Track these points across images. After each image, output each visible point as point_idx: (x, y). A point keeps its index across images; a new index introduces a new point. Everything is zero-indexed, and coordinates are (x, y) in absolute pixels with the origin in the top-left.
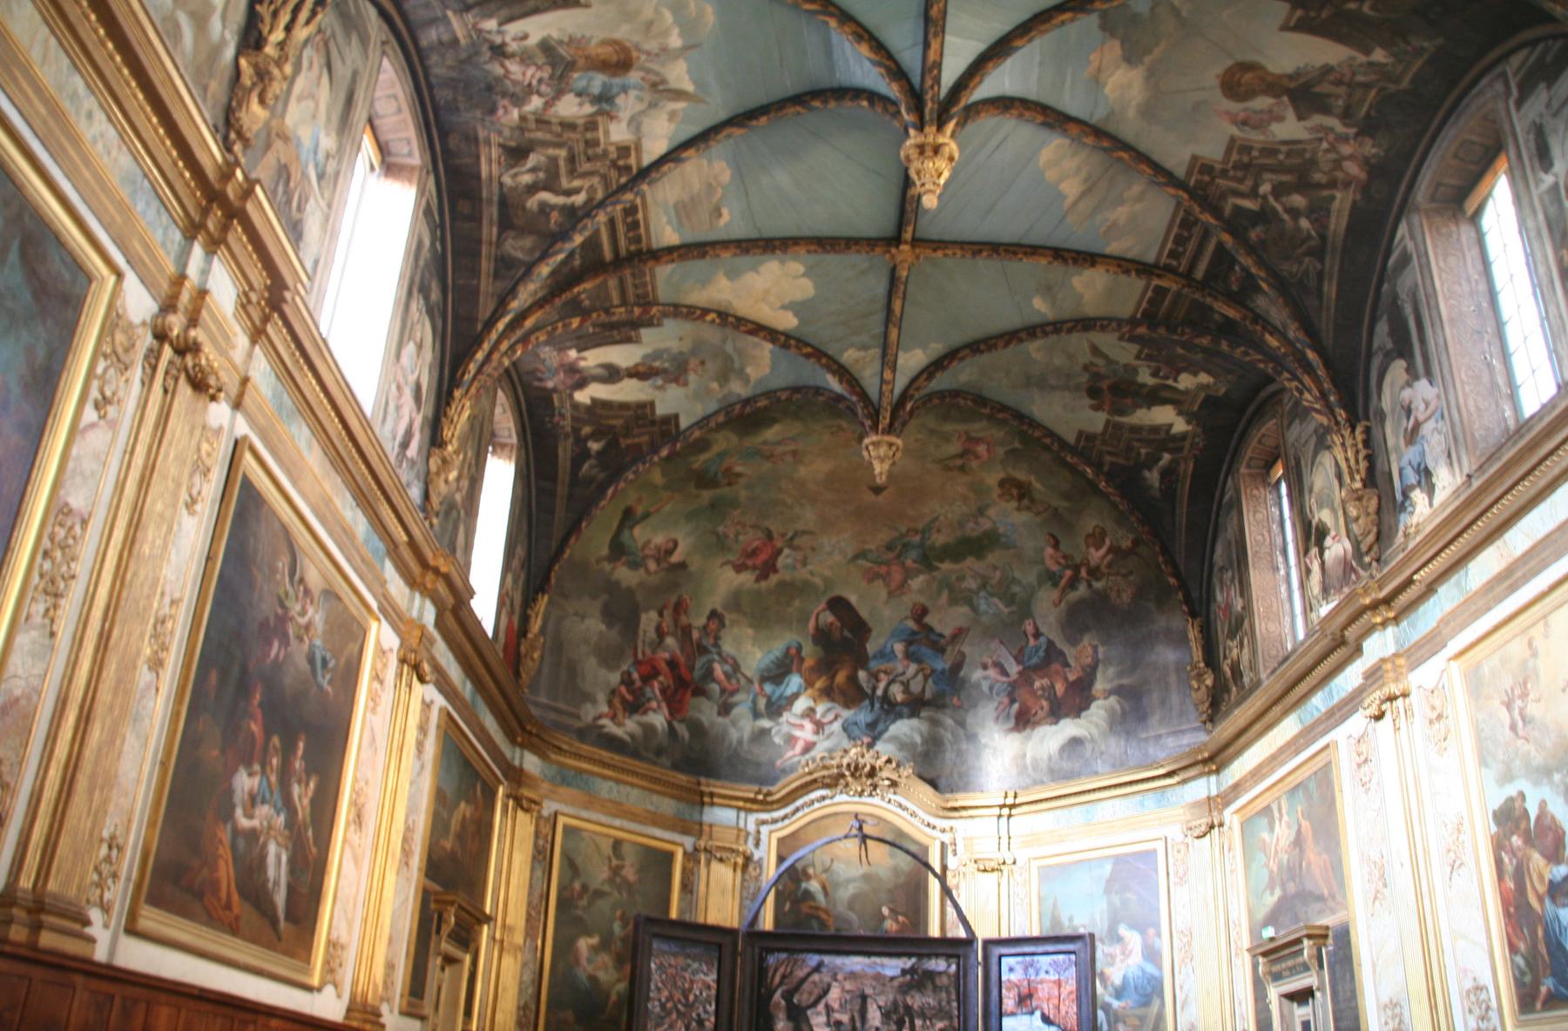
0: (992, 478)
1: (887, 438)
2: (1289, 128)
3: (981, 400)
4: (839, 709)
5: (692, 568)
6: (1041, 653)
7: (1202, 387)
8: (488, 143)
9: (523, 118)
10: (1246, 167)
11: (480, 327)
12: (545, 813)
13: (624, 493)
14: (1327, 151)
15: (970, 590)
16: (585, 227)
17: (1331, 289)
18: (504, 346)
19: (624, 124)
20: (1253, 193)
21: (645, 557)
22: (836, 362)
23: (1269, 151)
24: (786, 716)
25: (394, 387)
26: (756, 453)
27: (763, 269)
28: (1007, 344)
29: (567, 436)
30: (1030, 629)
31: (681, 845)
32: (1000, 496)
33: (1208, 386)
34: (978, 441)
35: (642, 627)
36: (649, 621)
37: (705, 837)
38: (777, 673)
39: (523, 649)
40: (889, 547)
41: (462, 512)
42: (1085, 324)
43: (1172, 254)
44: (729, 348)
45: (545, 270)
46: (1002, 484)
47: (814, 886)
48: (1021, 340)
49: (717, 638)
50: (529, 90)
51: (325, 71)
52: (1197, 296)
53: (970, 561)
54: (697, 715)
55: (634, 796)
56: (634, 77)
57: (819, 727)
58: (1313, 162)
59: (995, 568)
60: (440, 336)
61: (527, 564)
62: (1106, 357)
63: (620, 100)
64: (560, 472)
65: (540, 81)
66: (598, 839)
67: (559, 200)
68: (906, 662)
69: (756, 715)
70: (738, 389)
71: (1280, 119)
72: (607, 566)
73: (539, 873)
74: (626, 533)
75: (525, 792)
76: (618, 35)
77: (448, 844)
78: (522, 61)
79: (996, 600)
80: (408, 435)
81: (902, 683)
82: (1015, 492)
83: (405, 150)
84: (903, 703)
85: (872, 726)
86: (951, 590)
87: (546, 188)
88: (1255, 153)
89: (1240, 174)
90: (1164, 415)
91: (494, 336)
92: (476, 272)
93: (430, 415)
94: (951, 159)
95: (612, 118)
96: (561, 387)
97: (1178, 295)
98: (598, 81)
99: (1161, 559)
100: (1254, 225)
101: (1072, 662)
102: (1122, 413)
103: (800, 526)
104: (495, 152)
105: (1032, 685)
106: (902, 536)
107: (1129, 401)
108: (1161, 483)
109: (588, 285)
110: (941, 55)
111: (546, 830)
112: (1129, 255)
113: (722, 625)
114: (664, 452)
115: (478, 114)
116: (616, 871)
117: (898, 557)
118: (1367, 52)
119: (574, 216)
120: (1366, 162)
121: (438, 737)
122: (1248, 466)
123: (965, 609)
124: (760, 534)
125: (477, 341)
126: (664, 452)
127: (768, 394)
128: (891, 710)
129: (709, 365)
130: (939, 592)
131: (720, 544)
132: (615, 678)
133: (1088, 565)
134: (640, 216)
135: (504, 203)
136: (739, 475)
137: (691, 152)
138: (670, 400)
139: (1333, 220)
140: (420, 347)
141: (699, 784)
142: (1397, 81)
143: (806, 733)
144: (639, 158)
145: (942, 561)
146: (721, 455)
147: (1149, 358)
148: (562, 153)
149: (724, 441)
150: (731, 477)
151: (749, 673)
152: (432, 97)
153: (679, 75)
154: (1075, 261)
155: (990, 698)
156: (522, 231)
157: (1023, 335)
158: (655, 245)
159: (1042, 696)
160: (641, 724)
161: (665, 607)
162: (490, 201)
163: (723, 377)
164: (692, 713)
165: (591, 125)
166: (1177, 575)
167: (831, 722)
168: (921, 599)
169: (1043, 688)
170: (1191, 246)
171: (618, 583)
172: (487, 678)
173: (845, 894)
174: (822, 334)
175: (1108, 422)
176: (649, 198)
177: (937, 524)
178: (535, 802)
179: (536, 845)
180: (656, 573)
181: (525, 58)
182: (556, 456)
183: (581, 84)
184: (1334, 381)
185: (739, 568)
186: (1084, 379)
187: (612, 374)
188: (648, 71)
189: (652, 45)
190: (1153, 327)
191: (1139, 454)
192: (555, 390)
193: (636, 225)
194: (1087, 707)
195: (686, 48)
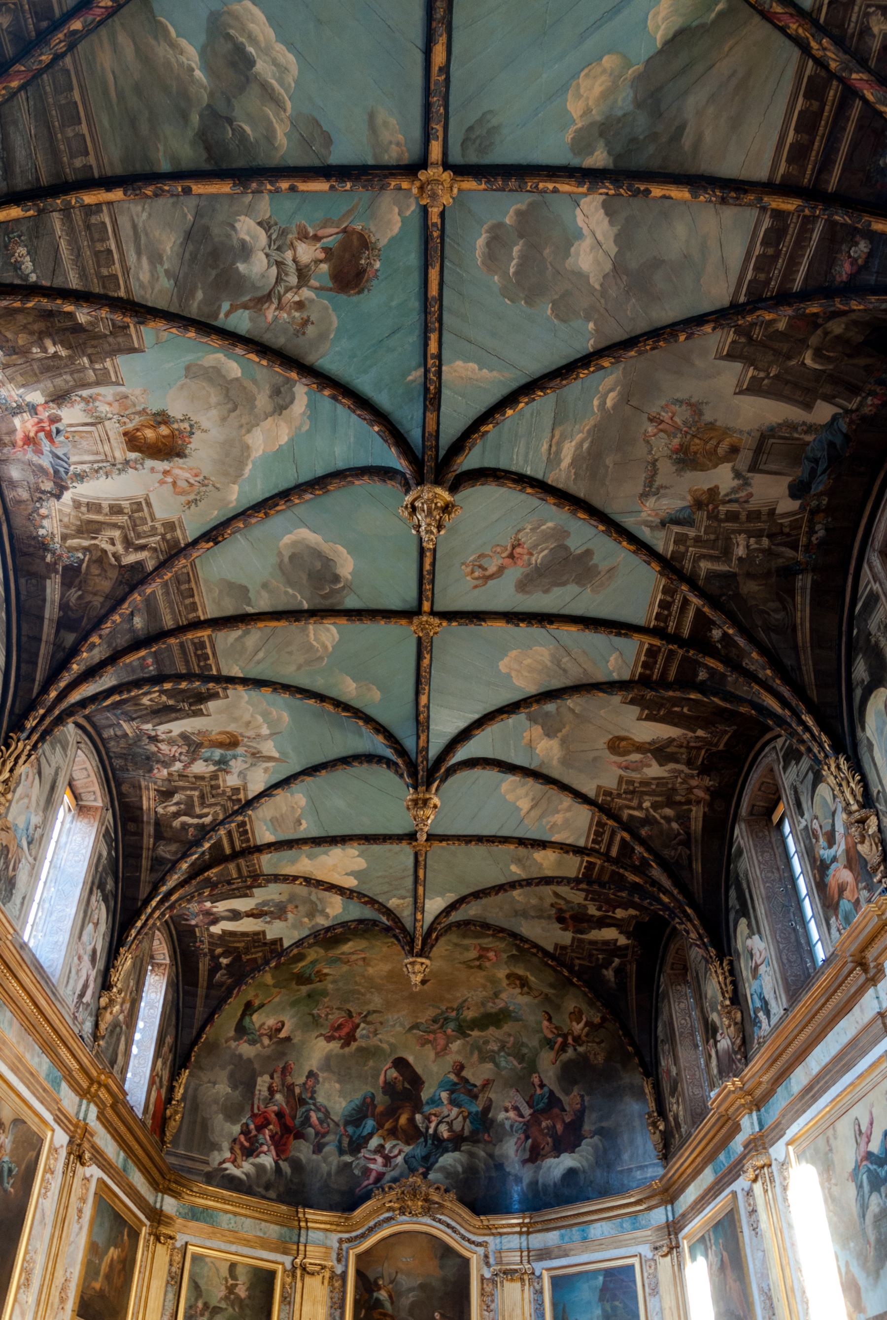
0: (501, 973)
1: (420, 960)
2: (655, 770)
3: (486, 926)
4: (401, 1146)
5: (295, 1041)
6: (546, 1101)
7: (632, 917)
8: (148, 788)
9: (170, 774)
10: (633, 792)
11: (139, 904)
12: (178, 1244)
13: (248, 992)
14: (682, 783)
15: (493, 1051)
16: (211, 838)
17: (698, 867)
18: (157, 914)
19: (236, 775)
20: (640, 807)
21: (263, 1035)
22: (385, 906)
23: (643, 783)
24: (363, 1152)
25: (76, 958)
26: (337, 960)
27: (331, 853)
28: (497, 894)
29: (205, 955)
30: (536, 1081)
31: (283, 1264)
32: (508, 985)
33: (636, 916)
34: (488, 950)
35: (258, 1088)
36: (263, 1083)
37: (301, 1257)
38: (356, 1118)
39: (168, 1112)
40: (435, 1021)
41: (124, 1027)
42: (547, 881)
43: (594, 841)
44: (313, 898)
45: (185, 866)
46: (508, 977)
47: (383, 1295)
48: (506, 891)
49: (314, 1092)
50: (174, 759)
51: (37, 777)
52: (614, 868)
53: (492, 1030)
54: (298, 1154)
55: (249, 1226)
56: (240, 750)
57: (388, 1159)
58: (674, 790)
59: (510, 1035)
60: (112, 913)
61: (174, 1048)
62: (564, 899)
63: (232, 763)
64: (200, 980)
65: (181, 754)
66: (218, 1263)
67: (195, 821)
68: (450, 1107)
69: (341, 1152)
70: (322, 922)
71: (649, 766)
72: (233, 1044)
73: (170, 1296)
74: (247, 1019)
75: (164, 1230)
76: (229, 729)
77: (97, 1285)
78: (169, 743)
79: (511, 1058)
80: (85, 986)
81: (447, 1123)
82: (518, 982)
83: (92, 798)
84: (448, 1140)
85: (425, 1158)
86: (480, 1051)
87: (185, 815)
88: (636, 785)
89: (629, 796)
90: (609, 934)
91: (149, 910)
92: (138, 868)
93: (102, 968)
94: (435, 806)
95: (227, 772)
96: (201, 924)
97: (602, 868)
98: (218, 753)
99: (621, 1032)
100: (643, 826)
101: (567, 1108)
102: (582, 933)
103: (371, 1007)
104: (152, 794)
105: (540, 1125)
106: (443, 1013)
107: (585, 925)
108: (616, 976)
109: (214, 871)
110: (428, 742)
111: (178, 1258)
112: (568, 842)
113: (318, 1082)
114: (273, 964)
115: (141, 772)
116: (231, 1289)
117: (441, 1027)
118: (694, 732)
119: (204, 831)
120: (707, 789)
121: (94, 1202)
122: (672, 969)
123: (490, 1066)
124: (344, 1014)
125: (138, 914)
126: (273, 964)
127: (343, 924)
128: (439, 1145)
129: (300, 908)
130: (472, 1053)
131: (316, 1021)
132: (236, 1129)
133: (572, 1034)
134: (248, 827)
135: (157, 824)
136: (326, 975)
137: (279, 791)
138: (274, 930)
139: (693, 823)
140: (96, 924)
141: (297, 1212)
142: (716, 745)
143: (378, 1165)
144: (246, 795)
145: (472, 1030)
146: (313, 963)
147: (592, 900)
148: (196, 793)
149: (314, 954)
150: (322, 977)
151: (336, 1119)
152: (111, 764)
153: (269, 748)
154: (533, 846)
155: (511, 1135)
156: (170, 840)
157: (507, 887)
158: (259, 843)
159: (547, 1134)
160: (253, 1164)
161: (275, 1071)
162: (149, 823)
163: (311, 915)
164: (293, 1153)
165: (215, 777)
166: (632, 1043)
167: (396, 1156)
168: (459, 1058)
169: (547, 1127)
170: (606, 837)
171: (240, 1056)
172: (136, 1147)
173: (406, 1301)
174: (373, 889)
175: (573, 939)
176: (253, 817)
177: (466, 1004)
178: (171, 1238)
179: (170, 1272)
180: (269, 1046)
181: (171, 742)
182: (198, 969)
183: (208, 754)
184: (705, 929)
185: (329, 1039)
186: (553, 911)
187: (235, 915)
188: (249, 747)
189: (251, 734)
190: (590, 883)
191: (598, 959)
192: (196, 926)
193: (246, 832)
194: (579, 1145)
195: (272, 735)
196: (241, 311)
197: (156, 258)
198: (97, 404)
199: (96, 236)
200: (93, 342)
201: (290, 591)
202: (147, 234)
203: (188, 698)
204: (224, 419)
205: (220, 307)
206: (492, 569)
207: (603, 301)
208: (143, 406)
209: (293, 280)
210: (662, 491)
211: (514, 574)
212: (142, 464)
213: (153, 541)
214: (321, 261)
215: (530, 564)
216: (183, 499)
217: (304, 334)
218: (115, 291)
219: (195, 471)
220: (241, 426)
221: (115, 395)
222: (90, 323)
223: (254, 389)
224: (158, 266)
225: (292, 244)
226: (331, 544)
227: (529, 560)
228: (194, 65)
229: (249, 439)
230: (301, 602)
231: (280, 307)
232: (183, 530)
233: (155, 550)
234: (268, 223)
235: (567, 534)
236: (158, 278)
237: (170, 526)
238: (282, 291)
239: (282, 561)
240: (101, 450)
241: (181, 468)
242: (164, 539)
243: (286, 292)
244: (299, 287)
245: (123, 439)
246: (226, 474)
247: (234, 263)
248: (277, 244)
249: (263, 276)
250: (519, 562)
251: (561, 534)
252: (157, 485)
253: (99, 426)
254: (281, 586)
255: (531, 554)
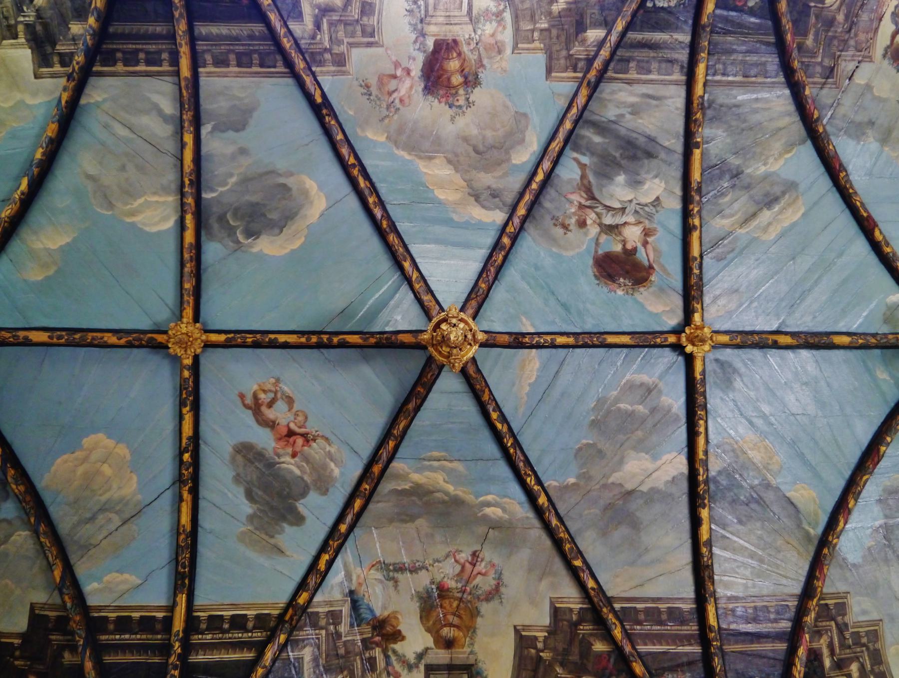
196: (579, 173)
197: (635, 111)
198: (494, 24)
199: (664, 65)
200: (563, 38)
201: (233, 180)
202: (657, 106)
203: (45, 26)
204: (466, 139)
205: (584, 154)
206: (270, 414)
207: (597, 487)
208: (488, 66)
209: (608, 220)
210: (391, 583)
211: (265, 440)
212: (419, 49)
213: (324, 38)
214: (624, 245)
215: (279, 456)
216: (373, 82)
217: (555, 225)
218: (614, 69)
219: (407, 101)
220: (456, 155)
221: (503, 43)
222: (584, 40)
223: (498, 173)
224: (629, 110)
225: (641, 223)
226: (306, 232)
227: (285, 454)
228: (768, 166)
229: (440, 161)
230: (212, 190)
231: (581, 207)
232: (334, 74)
233: (313, 37)
234: (658, 205)
235: (325, 492)
236: (618, 107)
237: (340, 61)
238: (597, 210)
239: (280, 175)
240: (438, 13)
241: (411, 88)
242: (326, 50)
243: (597, 214)
244: (600, 225)
245: (450, 37)
246: (400, 130)
247: (625, 173)
248: (641, 212)
249: (612, 196)
250: (283, 443)
251: (323, 484)
252: (394, 59)
253: (467, 19)
254: (242, 170)
255: (294, 455)
